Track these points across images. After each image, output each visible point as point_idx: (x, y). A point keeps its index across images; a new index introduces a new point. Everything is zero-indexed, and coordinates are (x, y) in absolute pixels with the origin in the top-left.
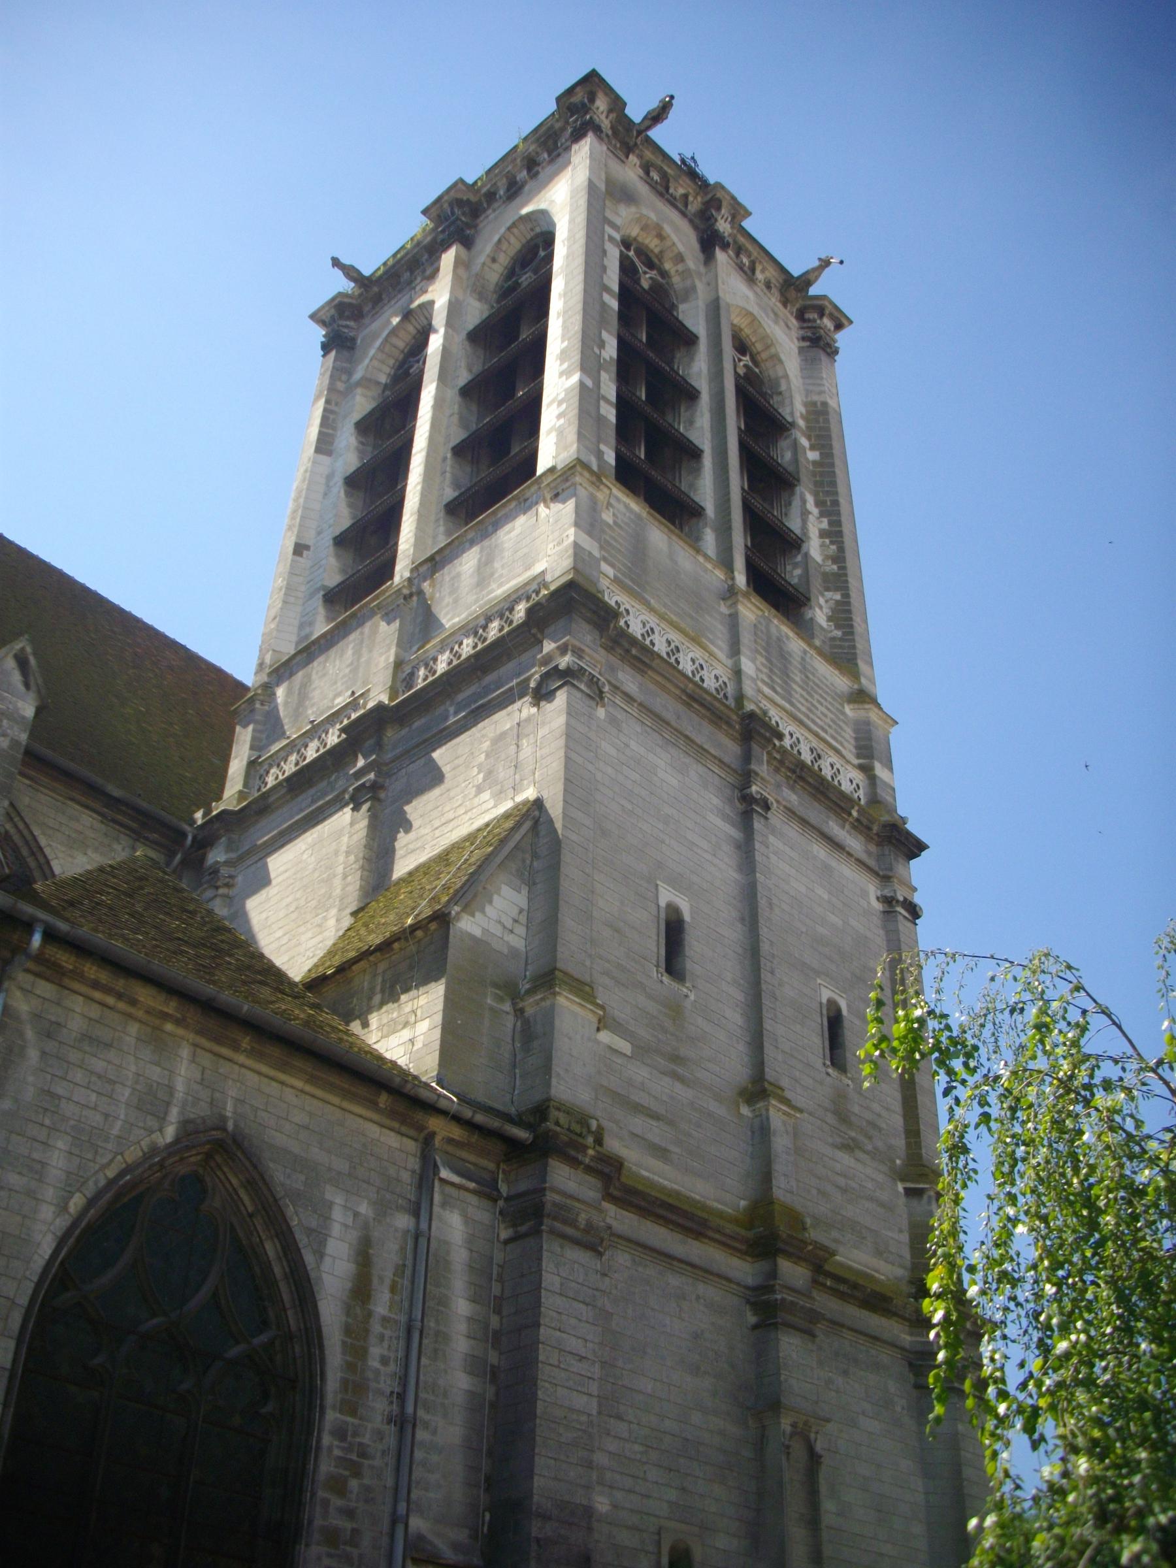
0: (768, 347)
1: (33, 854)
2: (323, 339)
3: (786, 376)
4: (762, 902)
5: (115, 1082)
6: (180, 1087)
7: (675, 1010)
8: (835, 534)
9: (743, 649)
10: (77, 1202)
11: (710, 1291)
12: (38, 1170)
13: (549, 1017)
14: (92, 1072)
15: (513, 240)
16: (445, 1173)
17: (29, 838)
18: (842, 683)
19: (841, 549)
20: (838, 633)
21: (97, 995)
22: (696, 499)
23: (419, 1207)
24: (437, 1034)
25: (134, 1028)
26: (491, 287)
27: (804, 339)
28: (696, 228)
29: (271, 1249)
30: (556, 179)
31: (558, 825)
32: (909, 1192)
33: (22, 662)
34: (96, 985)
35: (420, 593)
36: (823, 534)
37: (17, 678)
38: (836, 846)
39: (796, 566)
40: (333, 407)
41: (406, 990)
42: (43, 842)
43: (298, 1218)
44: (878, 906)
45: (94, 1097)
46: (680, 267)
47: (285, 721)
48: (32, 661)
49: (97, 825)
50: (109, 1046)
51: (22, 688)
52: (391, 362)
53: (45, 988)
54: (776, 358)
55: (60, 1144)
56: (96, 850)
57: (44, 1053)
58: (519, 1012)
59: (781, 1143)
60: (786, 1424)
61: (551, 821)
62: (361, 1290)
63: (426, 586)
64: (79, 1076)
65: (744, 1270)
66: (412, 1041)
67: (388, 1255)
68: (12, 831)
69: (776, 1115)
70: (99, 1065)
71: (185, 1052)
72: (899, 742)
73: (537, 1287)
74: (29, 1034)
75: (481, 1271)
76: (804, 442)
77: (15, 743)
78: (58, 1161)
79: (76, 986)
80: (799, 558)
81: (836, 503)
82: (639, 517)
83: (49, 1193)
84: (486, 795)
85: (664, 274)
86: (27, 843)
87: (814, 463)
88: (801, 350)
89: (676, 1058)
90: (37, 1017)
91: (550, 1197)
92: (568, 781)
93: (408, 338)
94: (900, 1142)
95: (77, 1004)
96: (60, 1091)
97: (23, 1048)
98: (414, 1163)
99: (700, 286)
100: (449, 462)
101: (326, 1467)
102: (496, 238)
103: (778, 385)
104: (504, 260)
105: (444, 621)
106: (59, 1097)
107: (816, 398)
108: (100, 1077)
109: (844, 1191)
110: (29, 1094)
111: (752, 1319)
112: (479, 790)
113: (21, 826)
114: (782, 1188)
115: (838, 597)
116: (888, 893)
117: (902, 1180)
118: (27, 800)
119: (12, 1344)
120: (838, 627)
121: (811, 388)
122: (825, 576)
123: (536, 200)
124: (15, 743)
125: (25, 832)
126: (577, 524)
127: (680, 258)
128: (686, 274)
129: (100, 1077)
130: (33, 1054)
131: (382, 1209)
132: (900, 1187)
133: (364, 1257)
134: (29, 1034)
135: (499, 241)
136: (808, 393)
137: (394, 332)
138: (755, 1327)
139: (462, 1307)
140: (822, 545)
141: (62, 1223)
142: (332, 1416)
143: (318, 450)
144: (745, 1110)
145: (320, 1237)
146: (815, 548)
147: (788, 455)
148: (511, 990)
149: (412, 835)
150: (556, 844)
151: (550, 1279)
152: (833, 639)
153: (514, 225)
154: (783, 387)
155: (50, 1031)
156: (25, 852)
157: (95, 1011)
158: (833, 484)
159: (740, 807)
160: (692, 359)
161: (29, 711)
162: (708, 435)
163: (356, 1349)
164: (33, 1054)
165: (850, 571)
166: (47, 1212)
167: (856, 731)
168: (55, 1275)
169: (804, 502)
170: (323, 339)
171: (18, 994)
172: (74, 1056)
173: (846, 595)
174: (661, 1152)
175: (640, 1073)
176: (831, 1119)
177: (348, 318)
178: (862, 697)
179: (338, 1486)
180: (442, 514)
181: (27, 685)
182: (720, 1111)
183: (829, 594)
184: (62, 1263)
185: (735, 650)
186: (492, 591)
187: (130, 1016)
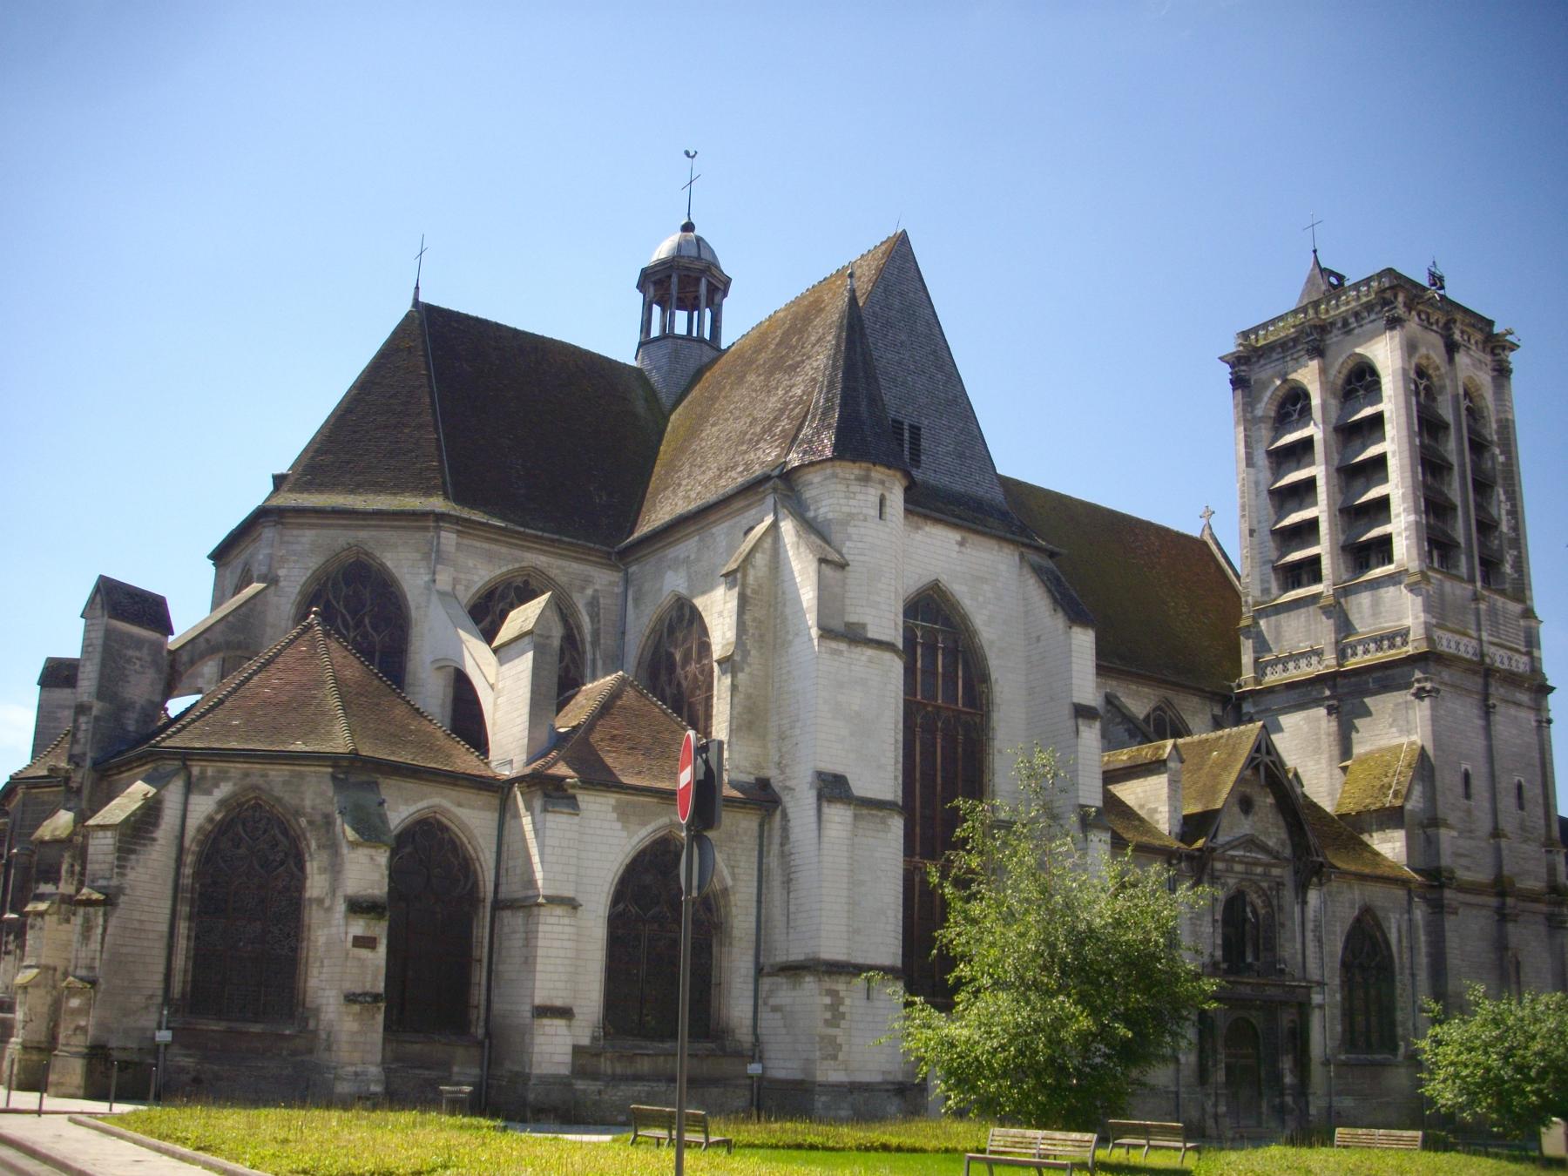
0: (1477, 390)
2: (1230, 377)
3: (1487, 407)
4: (1495, 753)
6: (1357, 897)
7: (1469, 812)
8: (1515, 513)
9: (1483, 628)
10: (1343, 939)
11: (1484, 912)
13: (1437, 835)
15: (1349, 362)
16: (1416, 899)
18: (1515, 608)
19: (1517, 523)
20: (1516, 576)
22: (1455, 536)
23: (1409, 911)
24: (1404, 849)
26: (1339, 388)
27: (1494, 370)
28: (1442, 335)
29: (1378, 934)
30: (1376, 339)
31: (1432, 759)
32: (1547, 851)
35: (1340, 603)
36: (1508, 513)
38: (1518, 704)
39: (1495, 538)
40: (1248, 433)
41: (1388, 828)
42: (1184, 717)
43: (1385, 925)
44: (1534, 724)
46: (1438, 373)
47: (1270, 642)
52: (1276, 403)
54: (1481, 396)
58: (1425, 833)
59: (1505, 853)
60: (1510, 953)
61: (1428, 757)
62: (1400, 941)
63: (1342, 600)
65: (1493, 901)
66: (1394, 849)
67: (1404, 927)
69: (1504, 843)
71: (1356, 887)
72: (1546, 634)
73: (1443, 930)
75: (1428, 924)
76: (1497, 451)
78: (1338, 929)
80: (1497, 534)
81: (1514, 492)
82: (1440, 580)
83: (1338, 939)
84: (1394, 730)
85: (1432, 383)
87: (1502, 464)
88: (1494, 378)
89: (1471, 831)
91: (1446, 902)
92: (1434, 740)
93: (1284, 391)
94: (1543, 831)
98: (1406, 897)
99: (1448, 382)
100: (1338, 518)
101: (1398, 991)
102: (1341, 360)
103: (1482, 412)
104: (1345, 372)
105: (1357, 627)
107: (1502, 416)
109: (1523, 859)
111: (1497, 918)
112: (1391, 726)
114: (1506, 872)
115: (1515, 553)
116: (1539, 718)
117: (1545, 846)
120: (1516, 572)
121: (1500, 408)
122: (1509, 539)
123: (1365, 346)
126: (1424, 611)
127: (1437, 368)
128: (1440, 377)
131: (1401, 915)
132: (1543, 850)
133: (1399, 931)
135: (1343, 363)
136: (1498, 412)
137: (1277, 388)
138: (1498, 921)
139: (1423, 938)
140: (1508, 520)
142: (1398, 977)
143: (1248, 465)
144: (1492, 841)
145: (1389, 928)
146: (1504, 528)
147: (1490, 464)
148: (1423, 826)
149: (1359, 735)
150: (1432, 769)
151: (1447, 926)
152: (1514, 579)
153: (1351, 355)
154: (1486, 414)
158: (1514, 485)
159: (1484, 708)
160: (1447, 441)
162: (1458, 493)
163: (1401, 958)
165: (1521, 537)
167: (1525, 632)
169: (1498, 495)
170: (1230, 377)
173: (1520, 552)
174: (1468, 869)
175: (1461, 842)
176: (1519, 832)
177: (1243, 365)
178: (1529, 613)
179: (1401, 996)
180: (1340, 552)
182: (1483, 844)
183: (1511, 552)
185: (1479, 630)
186: (1380, 623)
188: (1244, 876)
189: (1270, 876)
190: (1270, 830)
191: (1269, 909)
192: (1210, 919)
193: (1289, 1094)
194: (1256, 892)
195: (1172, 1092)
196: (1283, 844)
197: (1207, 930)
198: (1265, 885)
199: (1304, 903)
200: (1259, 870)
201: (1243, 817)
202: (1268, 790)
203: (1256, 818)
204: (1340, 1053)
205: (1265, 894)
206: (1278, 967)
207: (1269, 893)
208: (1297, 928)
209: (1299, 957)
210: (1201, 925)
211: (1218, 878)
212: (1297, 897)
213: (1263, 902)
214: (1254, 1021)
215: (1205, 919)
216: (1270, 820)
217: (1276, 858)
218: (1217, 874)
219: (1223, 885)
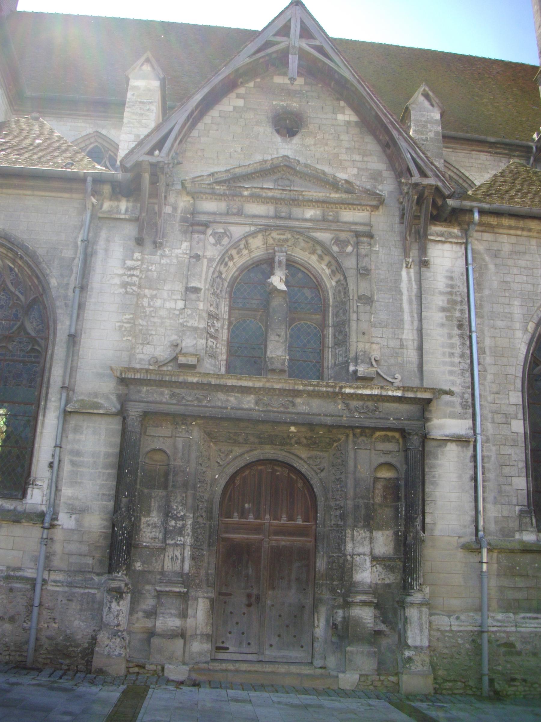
1: (465, 181)
5: (533, 269)
10: (531, 327)
12: (509, 317)
14: (521, 267)
17: (460, 174)
21: (512, 232)
25: (534, 242)
33: (426, 96)
34: (510, 227)
37: (426, 104)
42: (467, 174)
45: (525, 278)
48: (430, 93)
49: (489, 158)
50: (525, 253)
51: (430, 107)
53: (487, 236)
55: (516, 303)
56: (492, 169)
57: (496, 265)
64: (515, 270)
68: (452, 174)
70: (523, 263)
74: (487, 258)
77: (437, 133)
79: (501, 231)
83: (518, 326)
86: (460, 177)
90: (488, 250)
95: (504, 239)
96: (509, 279)
97: (486, 266)
106: (509, 282)
108: (525, 268)
110: (495, 285)
113: (455, 170)
118: (453, 158)
119: (520, 394)
124: (437, 133)
125: (458, 172)
129: (525, 268)
130: (492, 267)
134: (487, 258)
141: (528, 337)
155: (495, 255)
156: (461, 181)
157: (513, 240)
161: (438, 116)
164: (492, 267)
166: (519, 334)
168: (531, 360)
171: (476, 242)
172: (510, 262)
181: (432, 105)
184: (532, 354)
187: (530, 237)
188: (272, 222)
189: (337, 221)
190: (344, 157)
191: (339, 277)
192: (179, 287)
193: (364, 603)
194: (313, 252)
195: (27, 580)
196: (376, 177)
197: (170, 305)
198: (324, 236)
199: (424, 264)
200: (310, 213)
201: (278, 139)
202: (342, 103)
203: (310, 141)
204: (521, 530)
205: (327, 251)
206: (352, 368)
207: (335, 249)
208: (406, 306)
209: (411, 355)
210: (153, 297)
211: (206, 225)
212: (406, 254)
213: (329, 265)
214: (304, 468)
215: (168, 287)
216: (345, 144)
217: (347, 192)
218: (203, 218)
219: (219, 237)
